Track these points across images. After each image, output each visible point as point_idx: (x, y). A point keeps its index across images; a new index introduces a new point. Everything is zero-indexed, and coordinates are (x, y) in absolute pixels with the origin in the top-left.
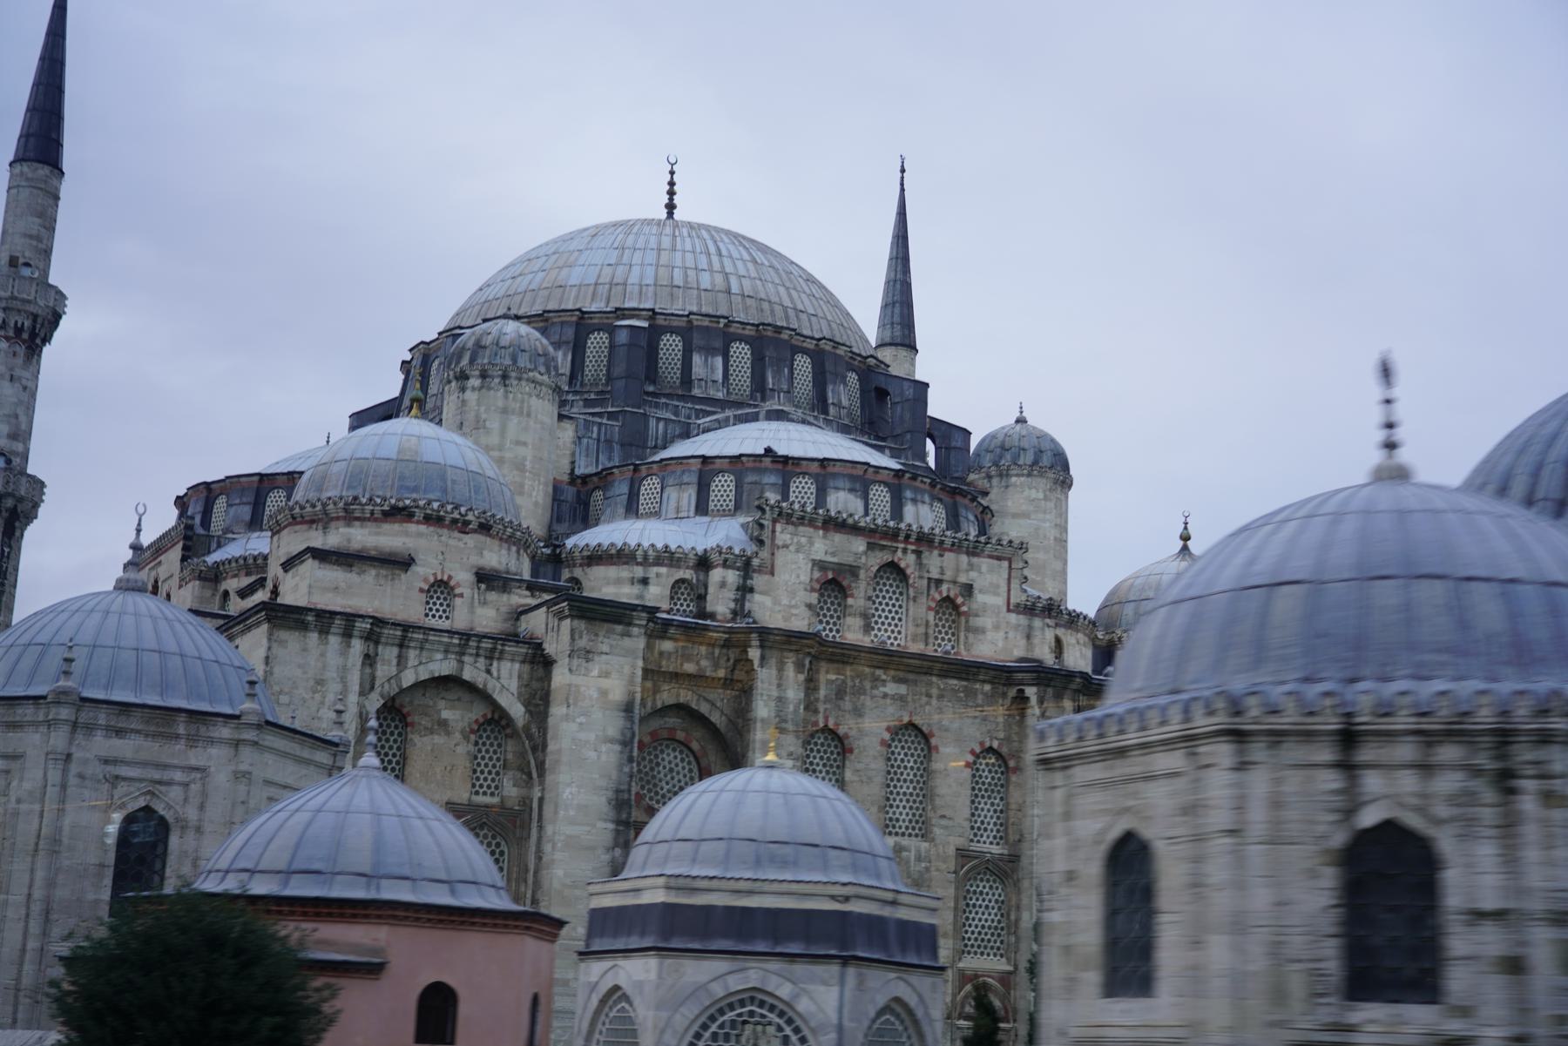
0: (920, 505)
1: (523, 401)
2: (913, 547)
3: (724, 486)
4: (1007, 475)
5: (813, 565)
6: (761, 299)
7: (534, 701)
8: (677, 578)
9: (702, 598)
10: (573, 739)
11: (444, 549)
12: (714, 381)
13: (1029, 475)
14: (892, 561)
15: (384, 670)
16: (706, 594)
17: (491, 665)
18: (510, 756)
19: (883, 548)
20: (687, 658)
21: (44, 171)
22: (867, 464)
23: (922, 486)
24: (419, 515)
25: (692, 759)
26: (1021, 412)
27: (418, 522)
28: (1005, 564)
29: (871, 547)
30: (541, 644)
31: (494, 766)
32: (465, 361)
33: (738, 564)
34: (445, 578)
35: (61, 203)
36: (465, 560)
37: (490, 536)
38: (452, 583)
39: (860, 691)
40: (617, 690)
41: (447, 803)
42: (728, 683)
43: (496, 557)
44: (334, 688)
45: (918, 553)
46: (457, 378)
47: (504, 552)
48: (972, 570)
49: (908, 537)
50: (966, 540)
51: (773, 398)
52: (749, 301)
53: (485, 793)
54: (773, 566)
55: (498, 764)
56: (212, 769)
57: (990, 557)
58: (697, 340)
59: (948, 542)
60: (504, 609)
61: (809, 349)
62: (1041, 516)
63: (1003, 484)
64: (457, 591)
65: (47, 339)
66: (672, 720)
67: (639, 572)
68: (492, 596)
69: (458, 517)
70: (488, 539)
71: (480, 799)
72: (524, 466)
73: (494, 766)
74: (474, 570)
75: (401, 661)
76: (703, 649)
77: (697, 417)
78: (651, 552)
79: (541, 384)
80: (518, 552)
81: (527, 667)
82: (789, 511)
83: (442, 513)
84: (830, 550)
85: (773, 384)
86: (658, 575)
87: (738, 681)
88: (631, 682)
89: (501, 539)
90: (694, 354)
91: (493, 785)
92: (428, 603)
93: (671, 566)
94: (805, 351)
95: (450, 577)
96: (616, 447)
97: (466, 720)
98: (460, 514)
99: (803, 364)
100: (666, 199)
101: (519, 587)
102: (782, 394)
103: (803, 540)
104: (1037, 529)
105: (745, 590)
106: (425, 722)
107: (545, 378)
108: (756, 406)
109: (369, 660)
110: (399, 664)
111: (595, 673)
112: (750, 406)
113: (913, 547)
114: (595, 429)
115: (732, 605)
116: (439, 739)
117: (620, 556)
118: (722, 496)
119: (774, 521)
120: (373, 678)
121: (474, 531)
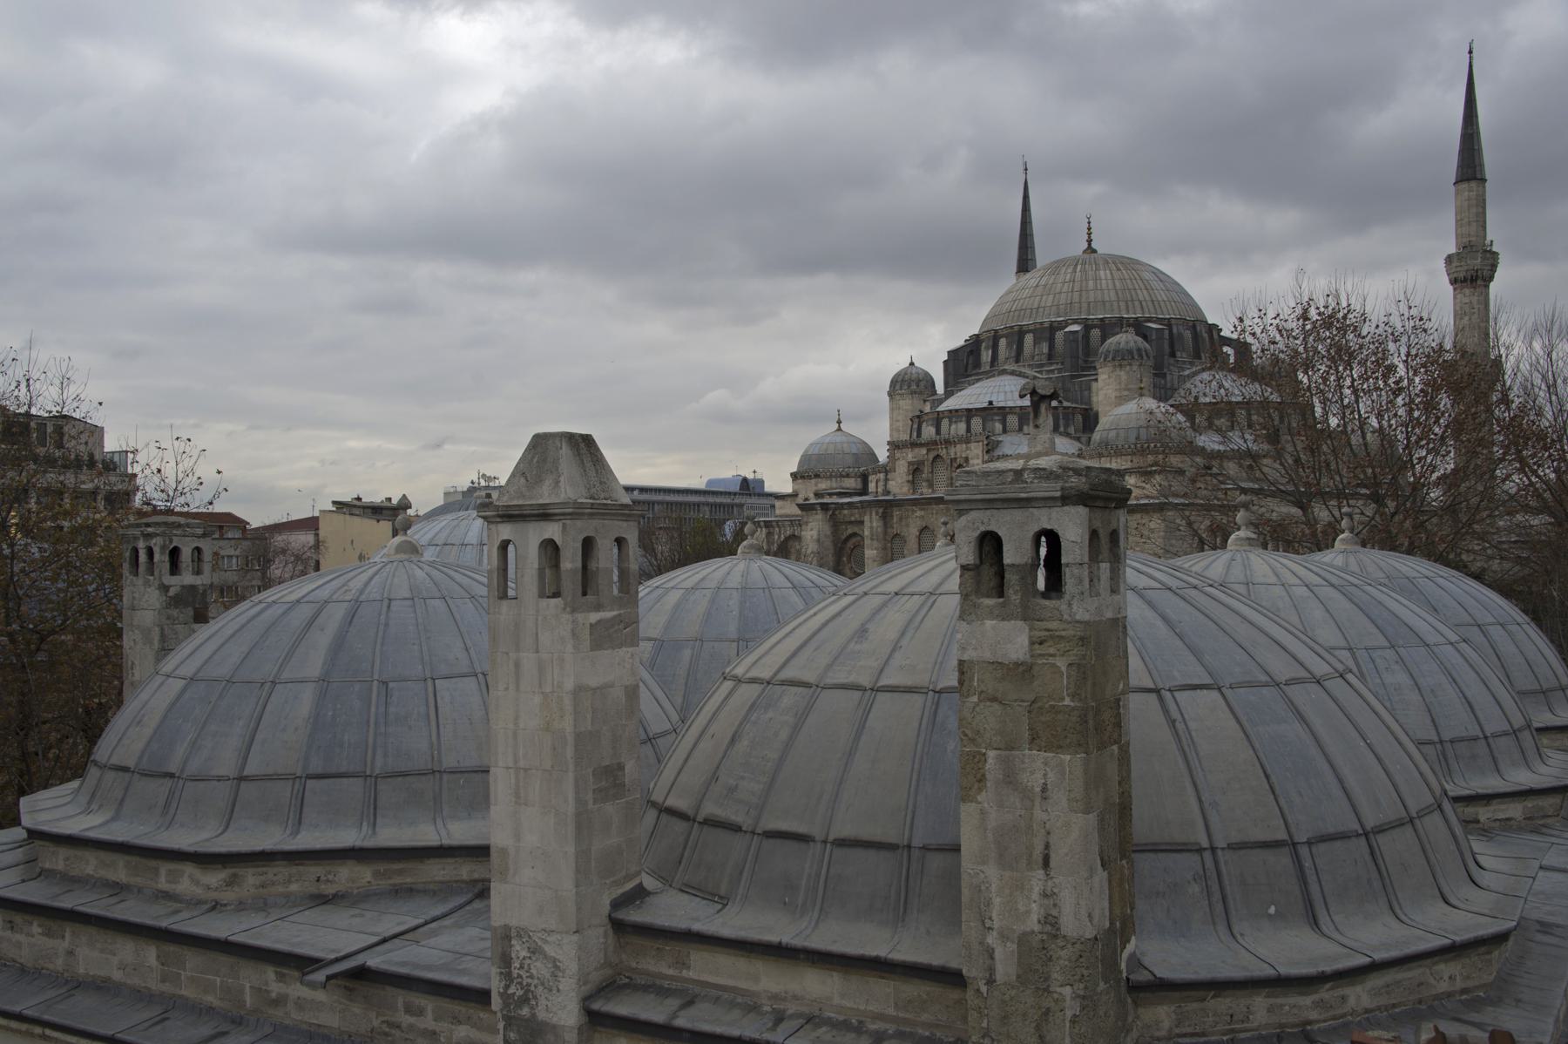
20: (852, 515)
29: (928, 450)
39: (907, 517)
100: (1086, 237)
105: (886, 480)
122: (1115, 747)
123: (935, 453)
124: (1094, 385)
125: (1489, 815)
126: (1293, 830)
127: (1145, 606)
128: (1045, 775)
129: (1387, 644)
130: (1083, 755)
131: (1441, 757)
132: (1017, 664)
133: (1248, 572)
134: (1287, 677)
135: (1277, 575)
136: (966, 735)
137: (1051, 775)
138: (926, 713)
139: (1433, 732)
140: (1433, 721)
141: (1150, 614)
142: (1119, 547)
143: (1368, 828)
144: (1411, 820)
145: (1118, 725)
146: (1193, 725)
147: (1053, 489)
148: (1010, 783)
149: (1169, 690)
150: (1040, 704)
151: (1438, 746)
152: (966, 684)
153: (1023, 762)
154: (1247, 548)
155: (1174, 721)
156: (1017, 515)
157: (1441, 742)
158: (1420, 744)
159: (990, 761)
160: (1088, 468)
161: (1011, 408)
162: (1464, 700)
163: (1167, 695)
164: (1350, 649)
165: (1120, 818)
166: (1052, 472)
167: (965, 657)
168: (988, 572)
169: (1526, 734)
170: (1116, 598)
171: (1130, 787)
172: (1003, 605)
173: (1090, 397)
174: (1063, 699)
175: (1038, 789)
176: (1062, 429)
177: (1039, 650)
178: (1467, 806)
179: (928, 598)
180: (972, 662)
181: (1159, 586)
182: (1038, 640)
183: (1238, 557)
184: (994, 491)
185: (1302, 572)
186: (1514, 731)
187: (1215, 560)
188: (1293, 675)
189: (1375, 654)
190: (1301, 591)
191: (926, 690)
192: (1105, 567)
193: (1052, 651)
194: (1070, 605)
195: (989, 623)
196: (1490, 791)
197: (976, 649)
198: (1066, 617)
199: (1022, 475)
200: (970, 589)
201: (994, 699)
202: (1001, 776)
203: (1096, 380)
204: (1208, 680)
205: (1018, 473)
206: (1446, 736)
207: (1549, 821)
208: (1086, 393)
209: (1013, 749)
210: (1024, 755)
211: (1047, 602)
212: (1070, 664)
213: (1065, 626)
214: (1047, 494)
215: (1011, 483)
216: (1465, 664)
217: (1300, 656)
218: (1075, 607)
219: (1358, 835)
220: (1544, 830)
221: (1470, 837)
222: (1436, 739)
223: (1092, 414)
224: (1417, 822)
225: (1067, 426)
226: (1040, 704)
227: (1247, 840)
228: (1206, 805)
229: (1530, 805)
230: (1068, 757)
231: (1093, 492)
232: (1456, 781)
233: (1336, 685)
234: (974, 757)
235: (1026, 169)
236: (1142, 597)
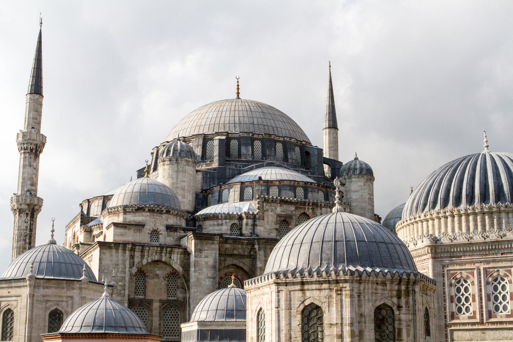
0: (314, 193)
1: (183, 168)
2: (311, 207)
3: (249, 191)
4: (351, 178)
5: (277, 216)
6: (264, 125)
7: (185, 267)
8: (232, 223)
9: (241, 229)
10: (197, 278)
11: (155, 220)
12: (248, 154)
13: (358, 178)
14: (304, 212)
15: (137, 260)
16: (242, 227)
17: (171, 256)
18: (179, 284)
19: (301, 208)
20: (234, 249)
21: (37, 96)
22: (295, 181)
24: (147, 210)
25: (239, 281)
26: (356, 156)
27: (147, 212)
29: (296, 208)
30: (186, 248)
31: (174, 288)
32: (165, 155)
33: (252, 217)
34: (156, 229)
35: (43, 106)
36: (162, 223)
37: (170, 214)
38: (158, 230)
40: (211, 261)
41: (160, 300)
42: (250, 256)
43: (172, 221)
44: (121, 266)
45: (313, 209)
46: (162, 162)
47: (175, 219)
49: (309, 204)
50: (329, 203)
51: (269, 158)
52: (261, 126)
53: (172, 296)
54: (263, 217)
55: (175, 287)
56: (74, 296)
58: (242, 141)
59: (323, 204)
60: (175, 237)
61: (281, 141)
62: (363, 191)
63: (350, 181)
64: (160, 233)
65: (41, 152)
66: (231, 269)
67: (220, 222)
68: (171, 233)
69: (159, 209)
70: (169, 215)
71: (170, 298)
72: (185, 189)
73: (174, 288)
74: (166, 226)
75: (142, 257)
76: (240, 246)
77: (243, 167)
78: (223, 215)
79: (189, 162)
80: (180, 219)
81: (183, 256)
82: (268, 199)
83: (154, 208)
84: (283, 210)
85: (269, 154)
86: (226, 223)
87: (252, 256)
88: (215, 259)
89: (174, 215)
90: (242, 146)
91: (174, 294)
92: (151, 237)
93: (230, 219)
94: (280, 141)
95: (158, 229)
96: (216, 180)
97: (164, 274)
98: (160, 208)
99: (279, 147)
101: (180, 230)
102: (272, 157)
103: (273, 208)
104: (362, 196)
105: (254, 225)
106: (151, 275)
107: (190, 159)
108: (263, 162)
109: (132, 257)
110: (141, 258)
111: (203, 256)
112: (261, 162)
113: (311, 207)
114: (209, 175)
115: (250, 231)
116: (156, 280)
117: (214, 217)
118: (248, 194)
119: (263, 202)
120: (134, 262)
121: (165, 213)
123: (302, 211)
235: (41, 23)
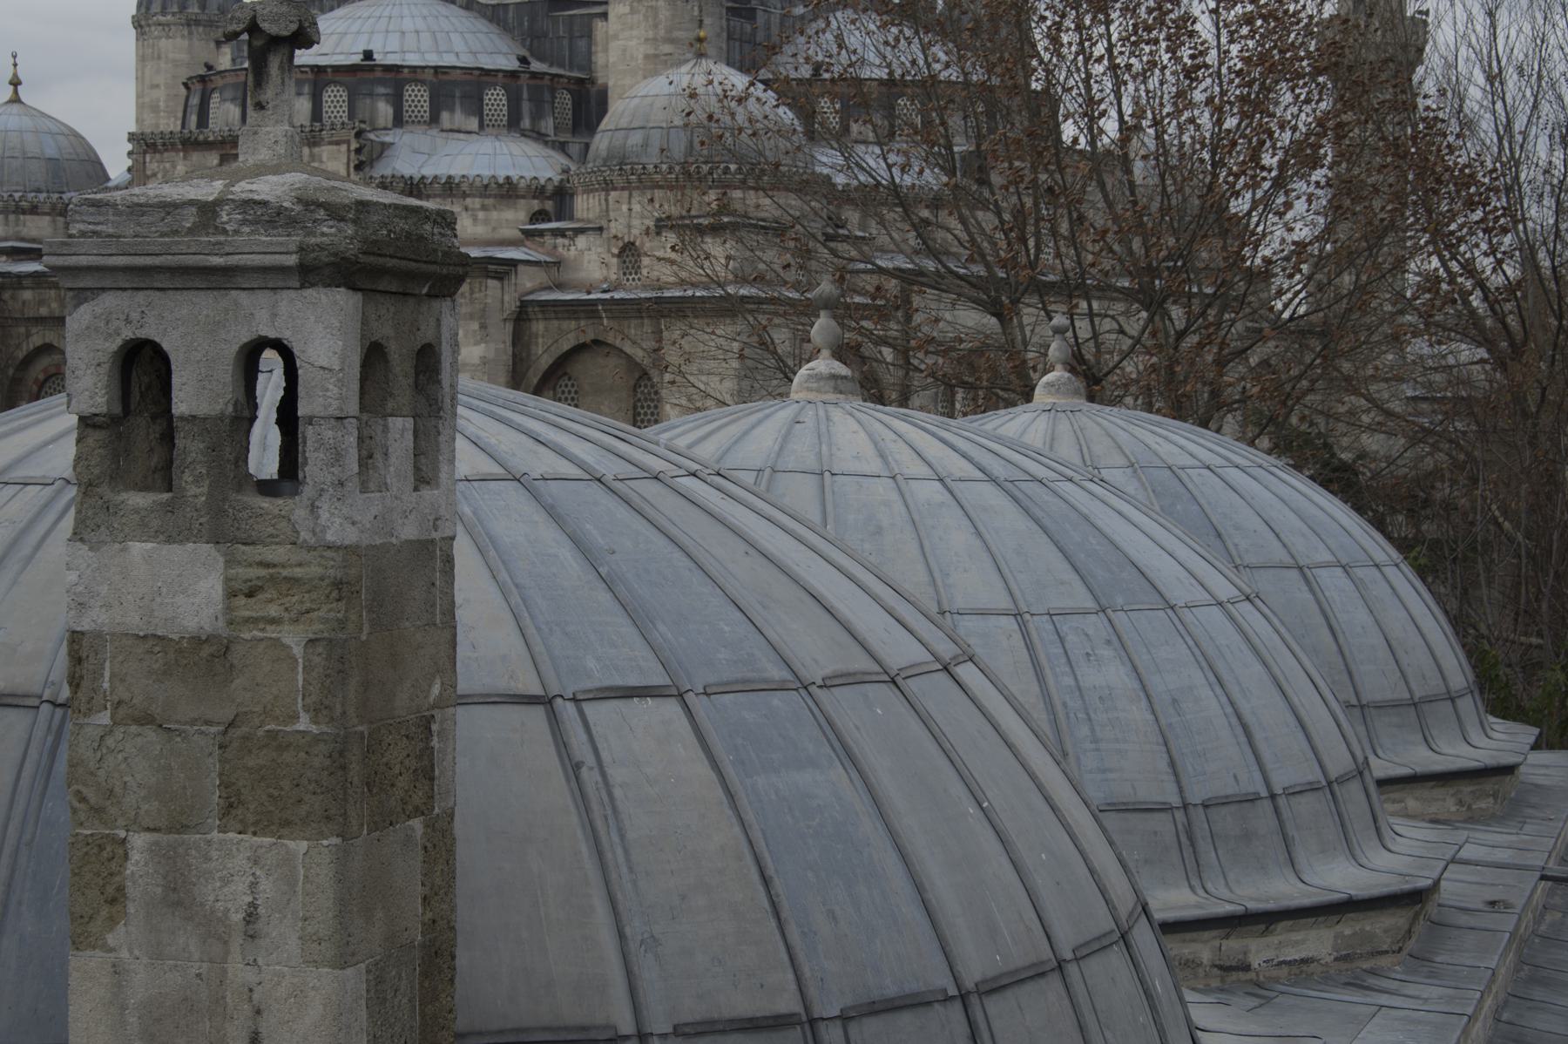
20: (41, 303)
23: (304, 76)
28: (344, 148)
48: (313, 161)
57: (330, 143)
72: (158, 106)
76: (53, 292)
79: (168, 25)
103: (168, 165)
119: (145, 153)
122: (417, 824)
124: (599, 25)
125: (1269, 954)
126: (812, 992)
127: (540, 517)
128: (253, 885)
129: (1090, 604)
130: (335, 840)
131: (1184, 839)
132: (198, 641)
133: (824, 447)
134: (828, 671)
135: (882, 456)
136: (83, 800)
137: (266, 885)
138: (33, 753)
139: (1171, 787)
140: (1172, 764)
141: (548, 533)
142: (439, 382)
143: (969, 985)
144: (1060, 966)
145: (426, 773)
146: (617, 774)
147: (281, 249)
148: (179, 903)
149: (574, 700)
150: (245, 729)
151: (1179, 815)
152: (84, 684)
153: (208, 859)
154: (831, 397)
155: (577, 767)
156: (204, 304)
157: (1185, 806)
158: (1098, 813)
159: (135, 856)
160: (362, 205)
161: (414, 69)
162: (1234, 720)
163: (568, 710)
164: (1017, 615)
165: (425, 975)
166: (280, 211)
167: (85, 625)
168: (143, 430)
169: (1355, 787)
170: (426, 492)
171: (453, 909)
172: (169, 508)
173: (590, 53)
174: (295, 717)
175: (237, 917)
176: (526, 123)
177: (244, 607)
178: (1227, 937)
179: (59, 492)
180: (98, 635)
181: (574, 471)
182: (245, 587)
183: (809, 415)
184: (156, 249)
185: (933, 449)
186: (1330, 784)
187: (760, 422)
188: (840, 667)
189: (1065, 625)
190: (930, 491)
191: (36, 702)
192: (400, 430)
193: (273, 611)
194: (313, 508)
195: (138, 548)
196: (1270, 906)
197: (107, 606)
198: (304, 535)
199: (215, 215)
200: (97, 471)
201: (146, 719)
202: (159, 890)
203: (605, 16)
204: (658, 678)
205: (208, 210)
206: (1196, 795)
207: (1384, 962)
208: (582, 43)
209: (184, 828)
210: (209, 843)
211: (265, 503)
212: (311, 641)
213: (304, 556)
214: (268, 260)
215: (191, 231)
216: (1244, 646)
217: (860, 627)
218: (324, 515)
219: (948, 999)
220: (1372, 981)
221: (1189, 996)
222: (1175, 800)
223: (593, 90)
224: (1072, 969)
225: (537, 116)
226: (245, 729)
227: (716, 1016)
228: (633, 946)
229: (1348, 932)
230: (303, 845)
231: (372, 259)
232: (1209, 886)
233: (933, 691)
234: (101, 848)
236: (536, 496)
